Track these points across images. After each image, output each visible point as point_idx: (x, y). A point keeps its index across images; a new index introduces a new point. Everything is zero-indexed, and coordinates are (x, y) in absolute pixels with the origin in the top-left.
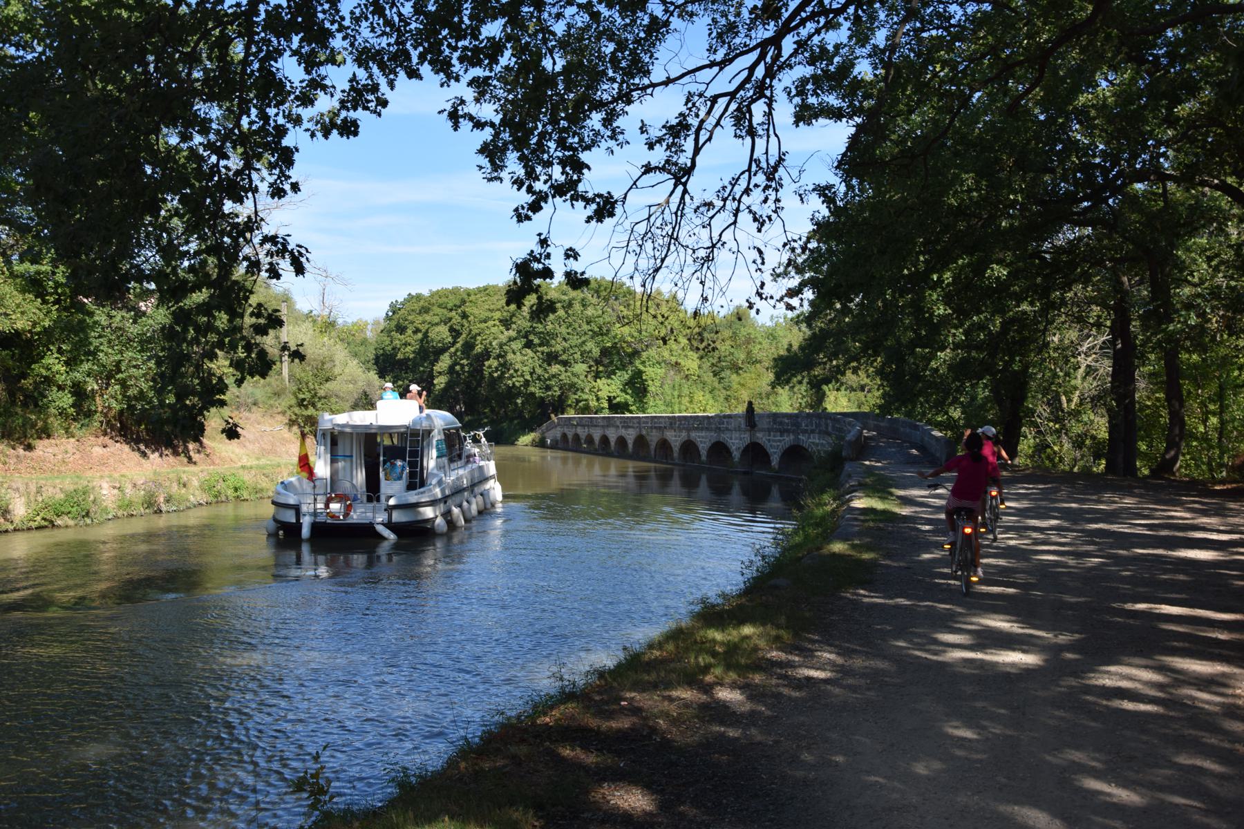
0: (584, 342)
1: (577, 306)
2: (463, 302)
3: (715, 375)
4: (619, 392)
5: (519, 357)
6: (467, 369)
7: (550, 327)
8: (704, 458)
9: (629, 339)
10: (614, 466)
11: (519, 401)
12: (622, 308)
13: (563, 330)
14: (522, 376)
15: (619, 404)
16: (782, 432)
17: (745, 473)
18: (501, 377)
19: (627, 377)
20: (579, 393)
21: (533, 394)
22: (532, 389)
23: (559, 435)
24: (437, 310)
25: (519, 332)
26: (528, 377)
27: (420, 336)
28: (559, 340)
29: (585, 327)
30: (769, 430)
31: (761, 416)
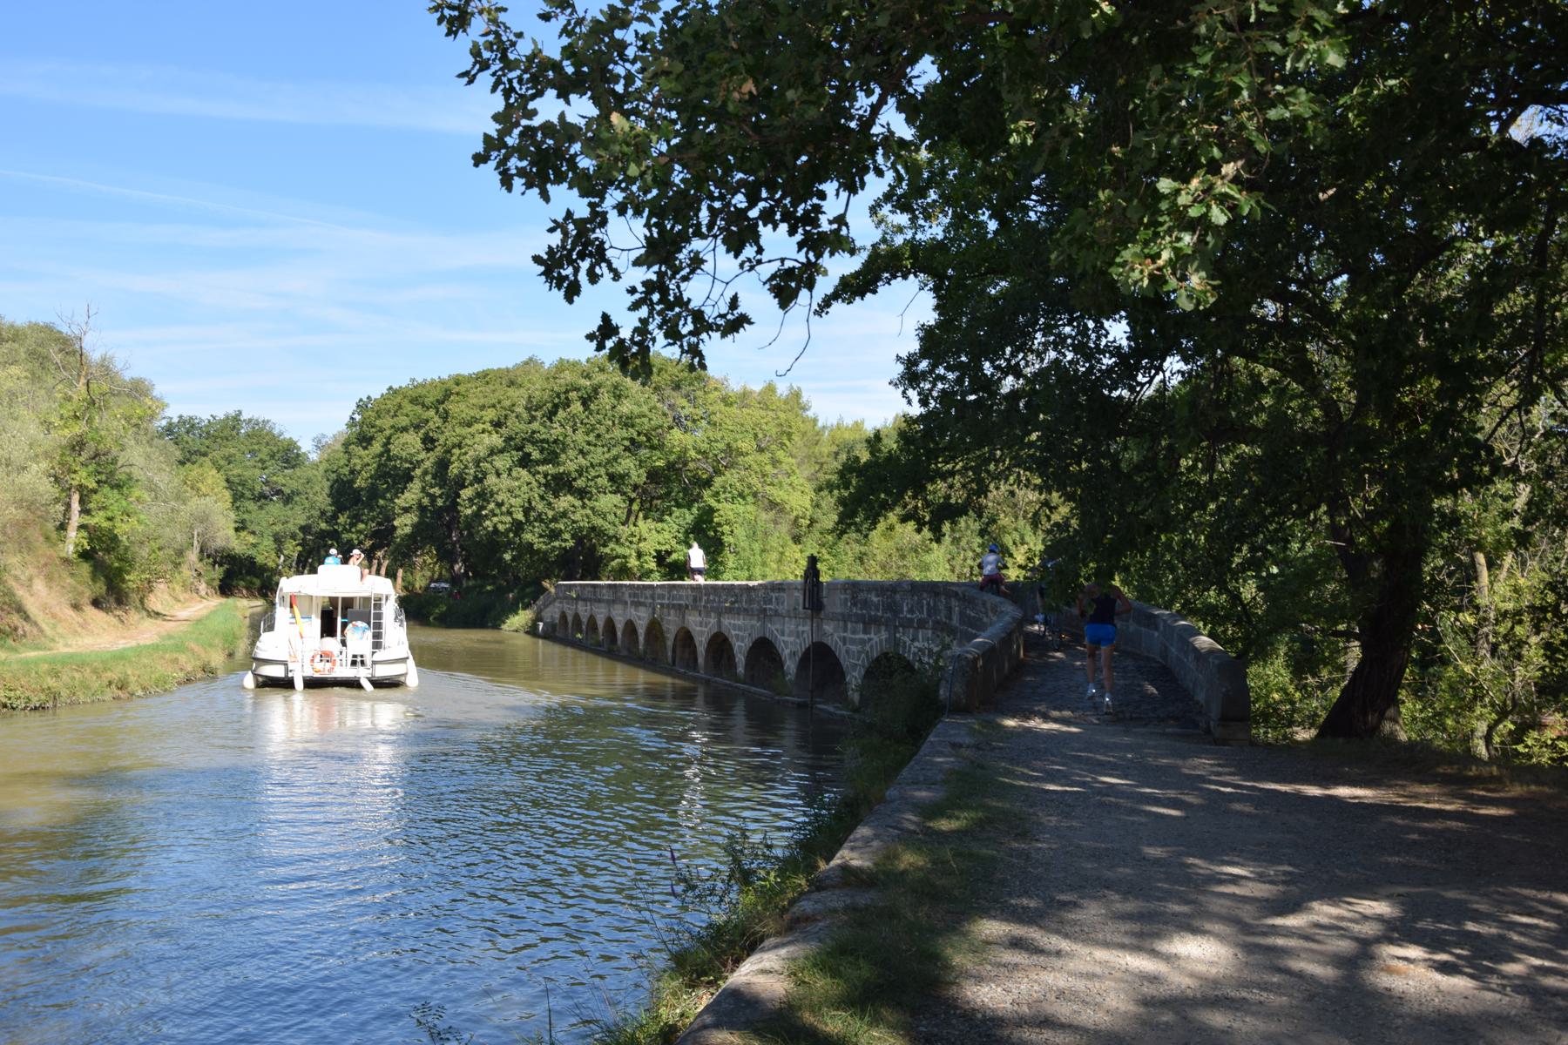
0: (616, 458)
1: (605, 399)
2: (447, 394)
4: (673, 542)
5: (506, 482)
6: (440, 502)
7: (556, 431)
8: (741, 669)
9: (693, 453)
10: (622, 674)
11: (507, 557)
12: (684, 402)
13: (580, 437)
14: (510, 513)
15: (675, 562)
16: (869, 623)
17: (800, 706)
18: (477, 515)
19: (689, 518)
20: (612, 545)
22: (527, 537)
23: (557, 616)
24: (408, 407)
25: (509, 439)
26: (520, 516)
27: (377, 447)
28: (571, 453)
29: (619, 433)
30: (845, 618)
31: (833, 586)
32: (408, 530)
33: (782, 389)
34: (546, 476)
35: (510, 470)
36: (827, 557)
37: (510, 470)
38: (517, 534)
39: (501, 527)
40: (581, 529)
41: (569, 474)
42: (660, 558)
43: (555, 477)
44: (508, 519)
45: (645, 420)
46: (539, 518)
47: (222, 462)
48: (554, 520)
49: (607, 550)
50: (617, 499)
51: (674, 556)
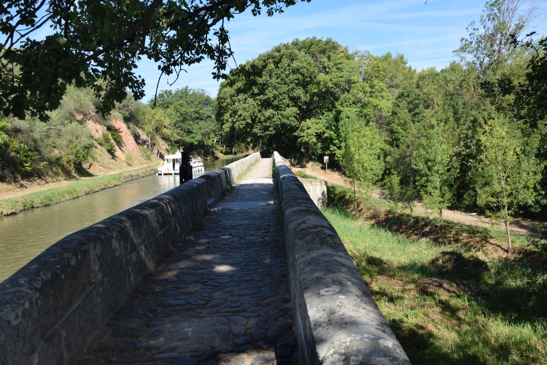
0: (293, 89)
1: (285, 61)
3: (410, 111)
4: (324, 128)
13: (274, 80)
14: (244, 120)
15: (326, 138)
19: (331, 116)
21: (256, 134)
22: (255, 130)
26: (249, 121)
29: (292, 77)
32: (228, 129)
33: (394, 56)
34: (261, 101)
35: (246, 99)
36: (401, 131)
37: (246, 99)
38: (252, 129)
39: (241, 127)
40: (277, 125)
41: (269, 99)
42: (319, 136)
43: (265, 101)
44: (244, 122)
45: (305, 70)
47: (178, 107)
48: (265, 121)
49: (296, 134)
50: (295, 109)
51: (326, 135)
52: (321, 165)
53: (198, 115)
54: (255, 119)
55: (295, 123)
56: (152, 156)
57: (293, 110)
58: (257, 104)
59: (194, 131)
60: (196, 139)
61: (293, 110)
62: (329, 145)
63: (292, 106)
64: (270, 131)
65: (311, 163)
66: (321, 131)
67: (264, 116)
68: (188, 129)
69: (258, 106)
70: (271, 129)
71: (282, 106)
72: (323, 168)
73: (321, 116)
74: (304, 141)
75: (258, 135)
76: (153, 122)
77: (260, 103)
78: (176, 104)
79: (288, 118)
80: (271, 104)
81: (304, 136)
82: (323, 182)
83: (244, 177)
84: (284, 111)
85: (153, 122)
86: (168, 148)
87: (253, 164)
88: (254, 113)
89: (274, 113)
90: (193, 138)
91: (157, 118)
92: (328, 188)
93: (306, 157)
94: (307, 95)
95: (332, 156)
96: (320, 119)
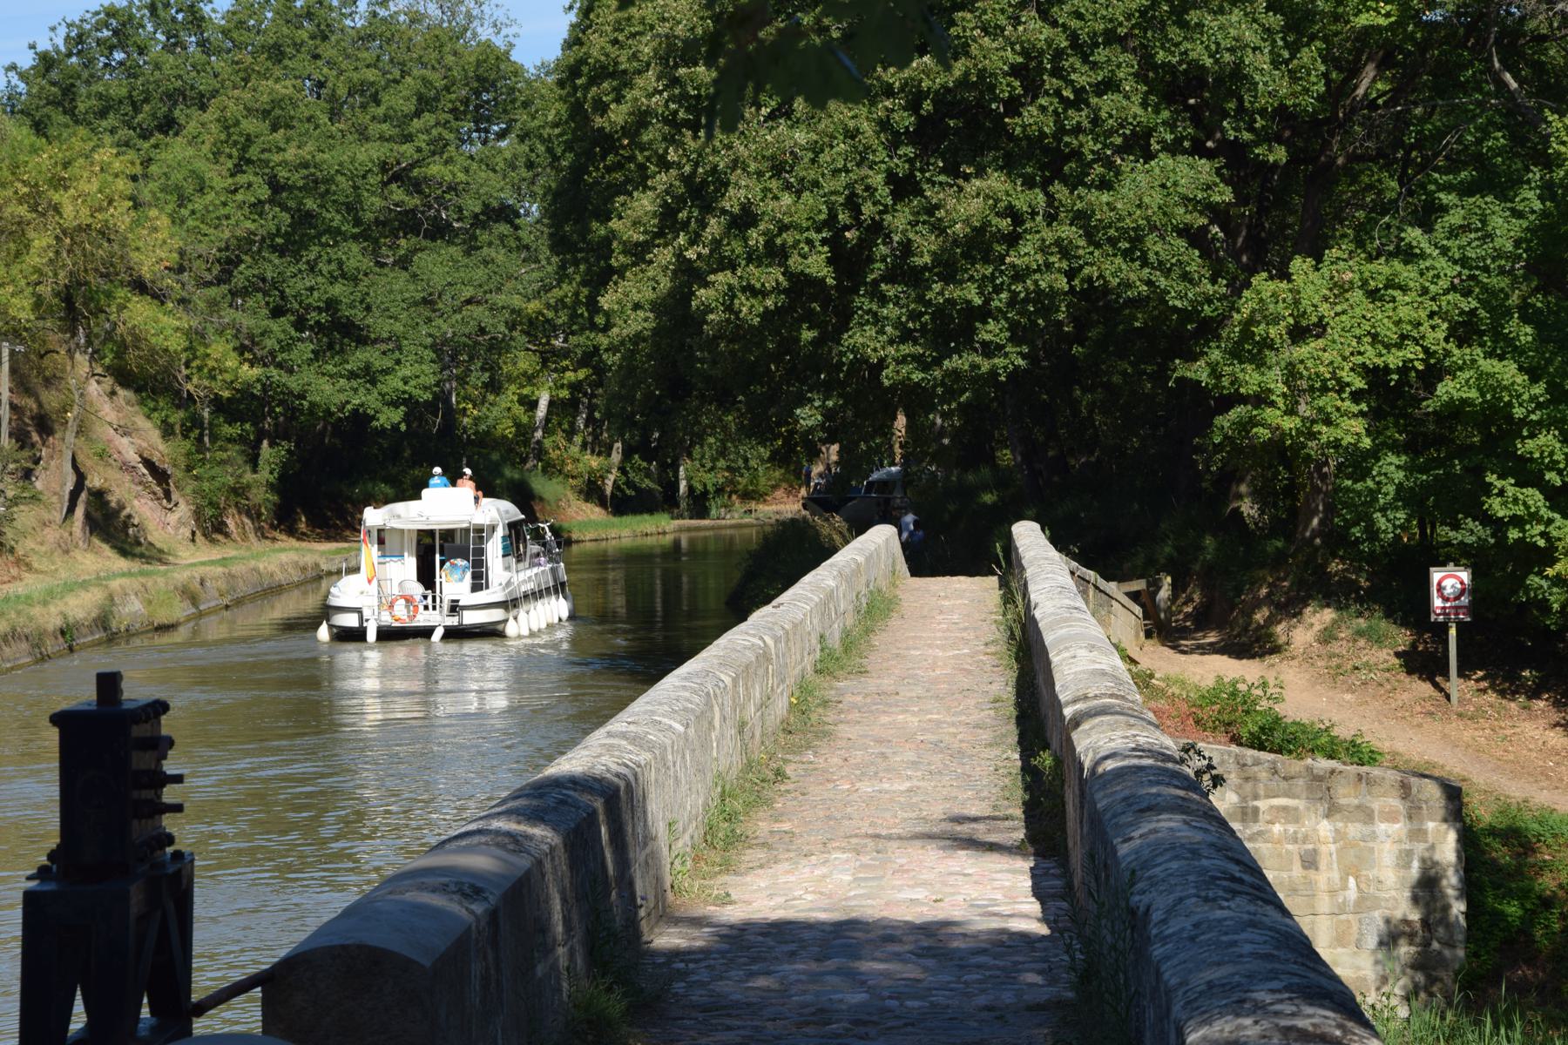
4: (1436, 336)
14: (775, 253)
15: (1455, 411)
19: (1505, 230)
22: (863, 339)
26: (817, 265)
32: (639, 322)
34: (913, 106)
39: (749, 309)
40: (1044, 301)
41: (984, 82)
42: (1388, 395)
43: (945, 100)
44: (772, 276)
46: (904, 271)
47: (250, 125)
48: (947, 269)
49: (1198, 372)
50: (1194, 175)
51: (1447, 389)
52: (1403, 638)
53: (414, 201)
54: (866, 243)
55: (1189, 286)
56: (26, 516)
57: (1171, 183)
58: (884, 125)
59: (380, 325)
60: (393, 383)
61: (1171, 183)
62: (1477, 472)
63: (1174, 149)
64: (989, 350)
65: (1320, 617)
66: (1411, 352)
67: (939, 229)
68: (331, 305)
69: (893, 146)
70: (991, 331)
71: (1090, 145)
72: (1423, 663)
73: (1414, 234)
74: (1263, 433)
75: (887, 377)
76: (41, 241)
77: (905, 121)
78: (231, 103)
79: (1133, 246)
80: (1001, 130)
81: (1261, 399)
82: (1432, 792)
83: (762, 826)
84: (1104, 185)
85: (41, 241)
86: (162, 450)
87: (841, 656)
88: (853, 204)
89: (1021, 204)
90: (369, 375)
91: (72, 212)
92: (1469, 840)
93: (1279, 560)
94: (1307, 55)
95: (1504, 565)
96: (1409, 255)
